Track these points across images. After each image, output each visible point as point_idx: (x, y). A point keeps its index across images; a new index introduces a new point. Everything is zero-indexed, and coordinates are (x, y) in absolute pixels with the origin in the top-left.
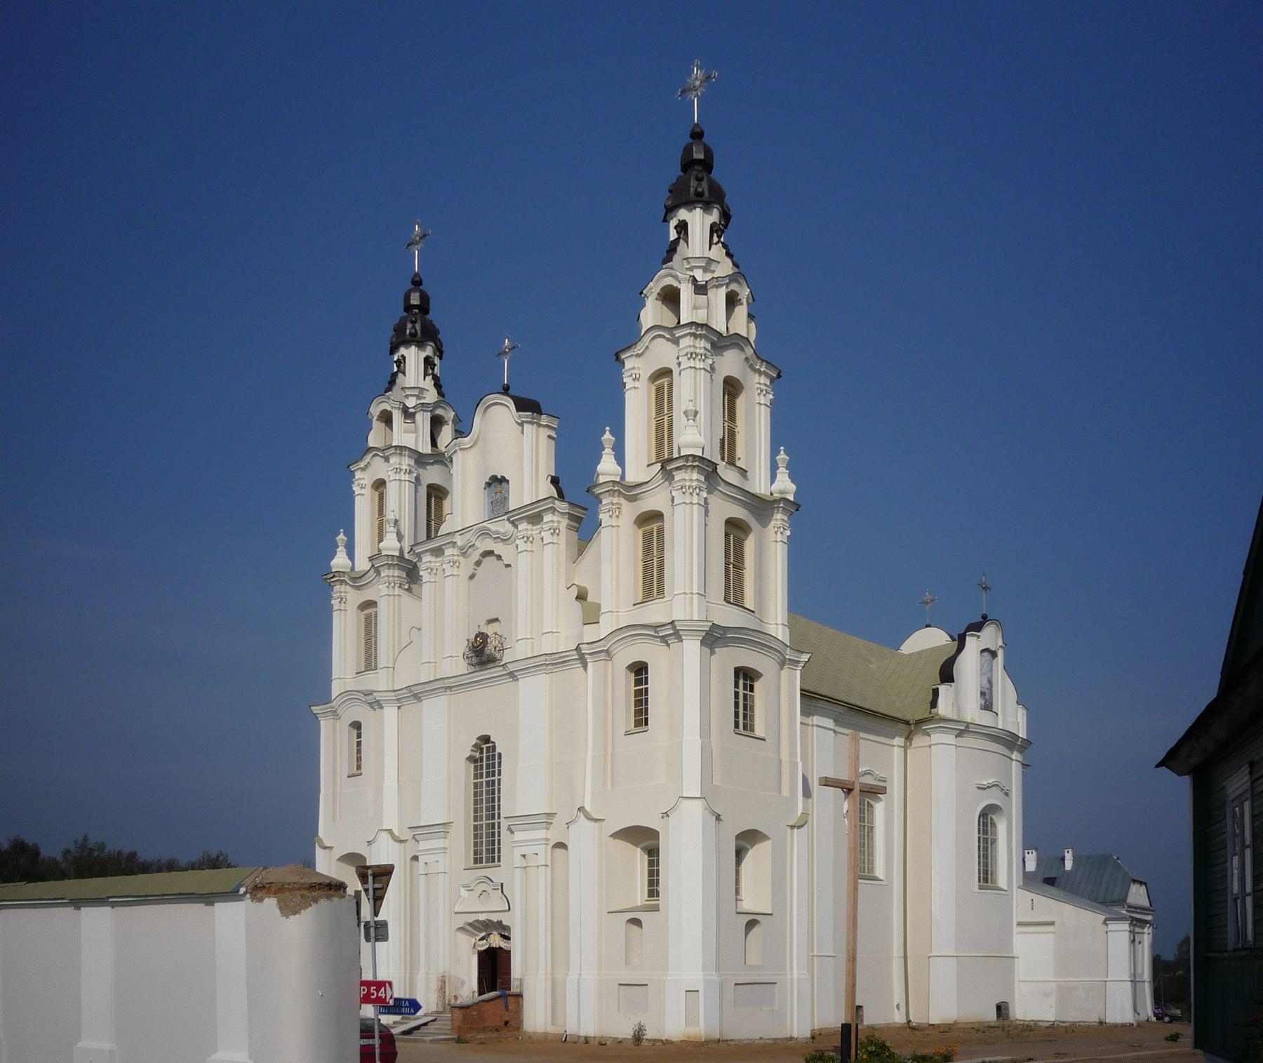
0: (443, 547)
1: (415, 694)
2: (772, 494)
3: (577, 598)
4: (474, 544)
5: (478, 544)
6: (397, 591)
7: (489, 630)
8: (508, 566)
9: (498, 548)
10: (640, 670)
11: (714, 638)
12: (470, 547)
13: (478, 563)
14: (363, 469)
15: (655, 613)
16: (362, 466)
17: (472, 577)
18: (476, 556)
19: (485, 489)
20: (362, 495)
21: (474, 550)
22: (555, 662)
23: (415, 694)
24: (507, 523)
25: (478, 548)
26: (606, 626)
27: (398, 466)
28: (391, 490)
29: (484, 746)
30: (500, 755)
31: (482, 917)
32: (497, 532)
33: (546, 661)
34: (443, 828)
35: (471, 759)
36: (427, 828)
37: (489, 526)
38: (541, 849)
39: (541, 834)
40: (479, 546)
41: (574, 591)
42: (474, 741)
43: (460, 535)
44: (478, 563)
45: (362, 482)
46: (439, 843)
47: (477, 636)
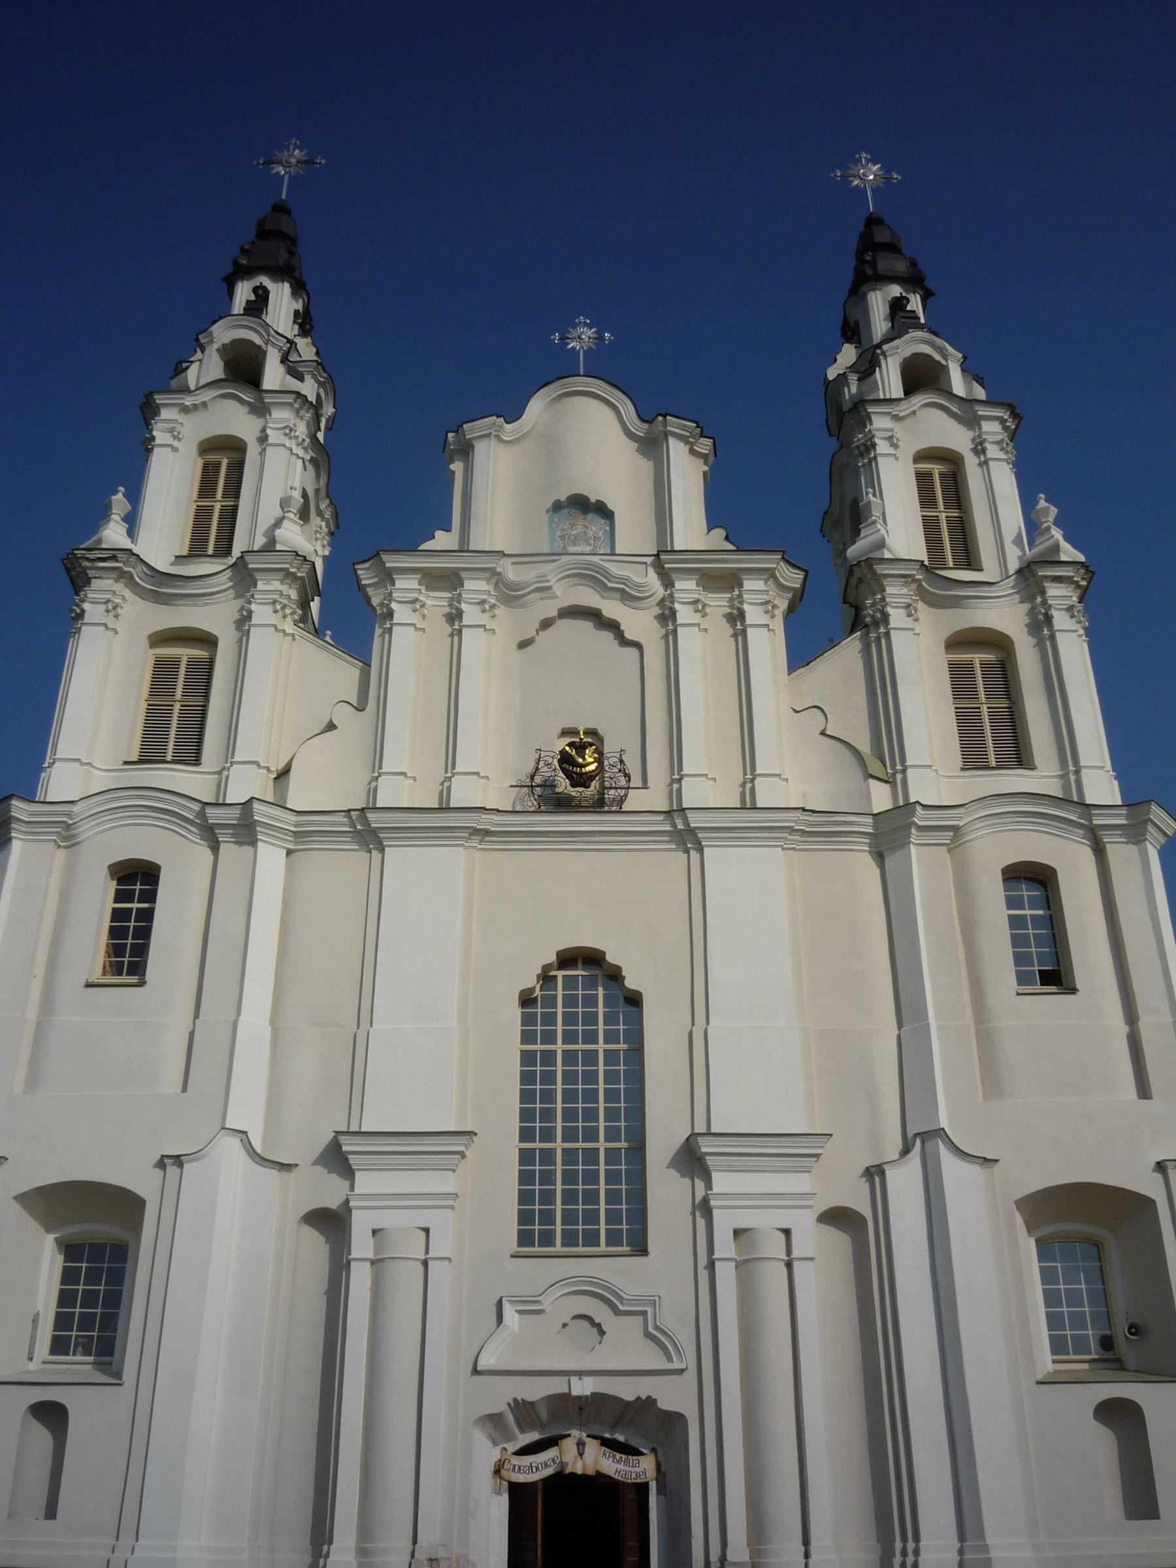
0: (463, 574)
4: (549, 588)
5: (558, 590)
6: (289, 627)
12: (538, 590)
13: (546, 624)
14: (185, 410)
16: (187, 403)
17: (524, 645)
18: (551, 609)
19: (548, 511)
20: (175, 450)
21: (542, 599)
24: (651, 570)
25: (556, 597)
27: (292, 426)
29: (560, 974)
31: (582, 1388)
32: (625, 581)
33: (796, 822)
35: (527, 1000)
36: (377, 1140)
37: (605, 564)
40: (558, 593)
43: (513, 564)
44: (546, 624)
45: (179, 428)
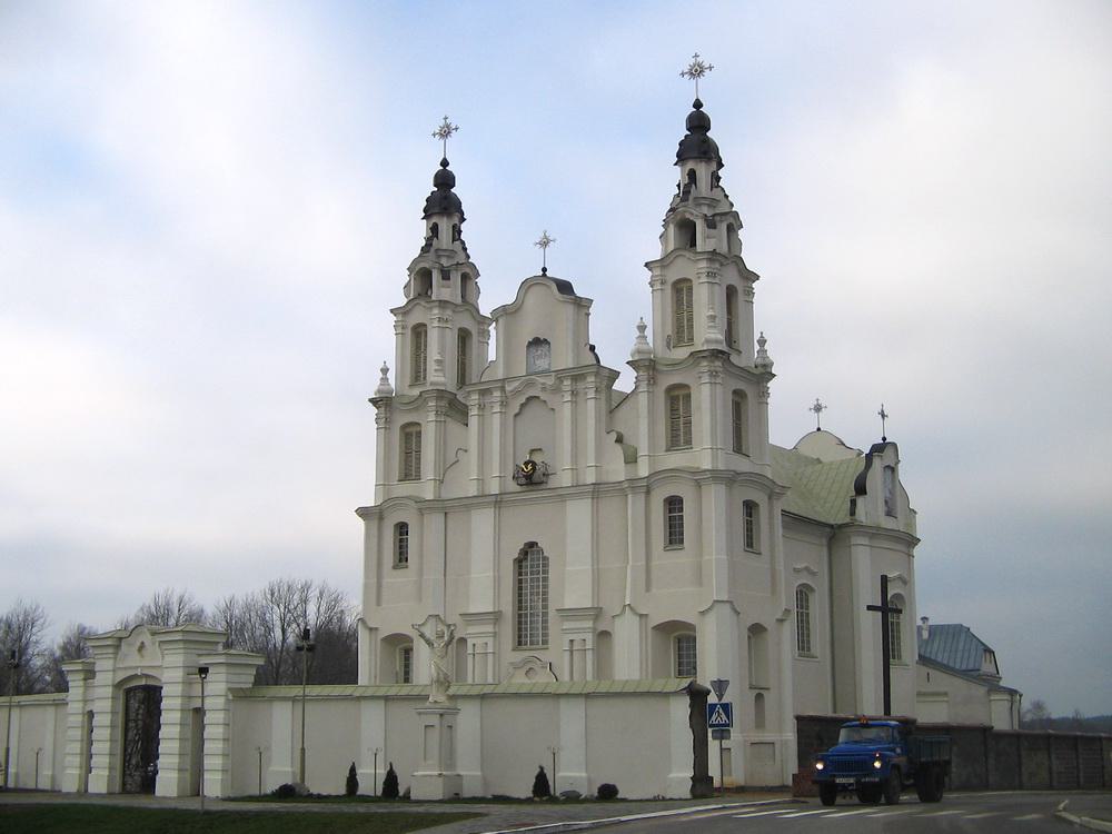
1: (468, 504)
2: (756, 367)
3: (616, 441)
7: (538, 459)
8: (553, 409)
9: (543, 396)
10: (674, 504)
11: (730, 479)
15: (676, 460)
22: (598, 491)
23: (468, 504)
26: (643, 470)
28: (433, 336)
30: (546, 559)
34: (496, 617)
38: (589, 637)
39: (590, 624)
41: (614, 436)
42: (522, 547)
44: (522, 405)
46: (490, 628)
47: (526, 464)
